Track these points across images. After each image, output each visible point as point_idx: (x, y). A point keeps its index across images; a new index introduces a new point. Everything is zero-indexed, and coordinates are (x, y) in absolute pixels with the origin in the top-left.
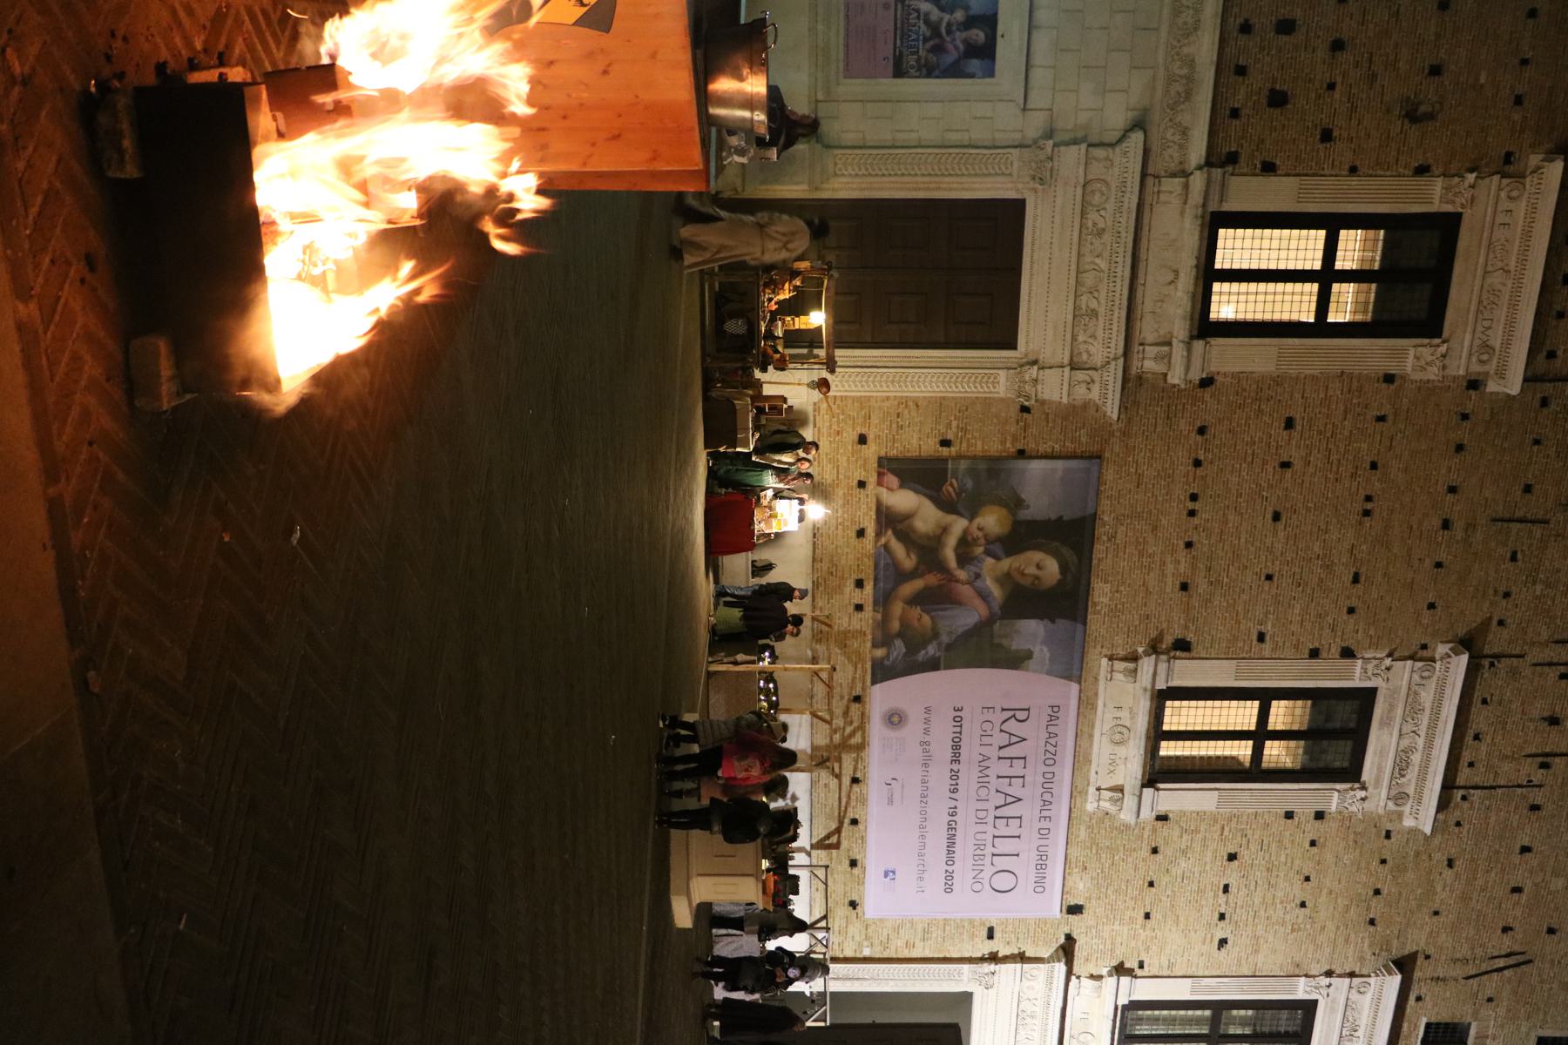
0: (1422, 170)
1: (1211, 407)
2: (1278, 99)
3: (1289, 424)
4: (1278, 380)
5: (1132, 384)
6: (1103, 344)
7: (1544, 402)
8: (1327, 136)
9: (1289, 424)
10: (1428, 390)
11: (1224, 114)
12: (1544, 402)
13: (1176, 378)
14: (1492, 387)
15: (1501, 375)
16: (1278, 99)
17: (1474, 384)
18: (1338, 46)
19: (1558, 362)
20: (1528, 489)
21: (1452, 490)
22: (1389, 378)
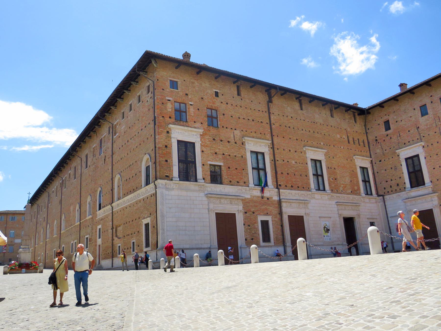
0: (401, 165)
1: (435, 180)
2: (398, 185)
3: (434, 168)
4: (429, 172)
5: (434, 192)
6: (428, 198)
7: (424, 137)
8: (400, 178)
9: (434, 168)
10: (426, 152)
11: (401, 191)
12: (424, 137)
13: (432, 186)
14: (423, 145)
15: (421, 145)
16: (398, 185)
17: (423, 147)
18: (391, 180)
19: (418, 138)
20: (435, 132)
21: (438, 142)
22: (425, 158)
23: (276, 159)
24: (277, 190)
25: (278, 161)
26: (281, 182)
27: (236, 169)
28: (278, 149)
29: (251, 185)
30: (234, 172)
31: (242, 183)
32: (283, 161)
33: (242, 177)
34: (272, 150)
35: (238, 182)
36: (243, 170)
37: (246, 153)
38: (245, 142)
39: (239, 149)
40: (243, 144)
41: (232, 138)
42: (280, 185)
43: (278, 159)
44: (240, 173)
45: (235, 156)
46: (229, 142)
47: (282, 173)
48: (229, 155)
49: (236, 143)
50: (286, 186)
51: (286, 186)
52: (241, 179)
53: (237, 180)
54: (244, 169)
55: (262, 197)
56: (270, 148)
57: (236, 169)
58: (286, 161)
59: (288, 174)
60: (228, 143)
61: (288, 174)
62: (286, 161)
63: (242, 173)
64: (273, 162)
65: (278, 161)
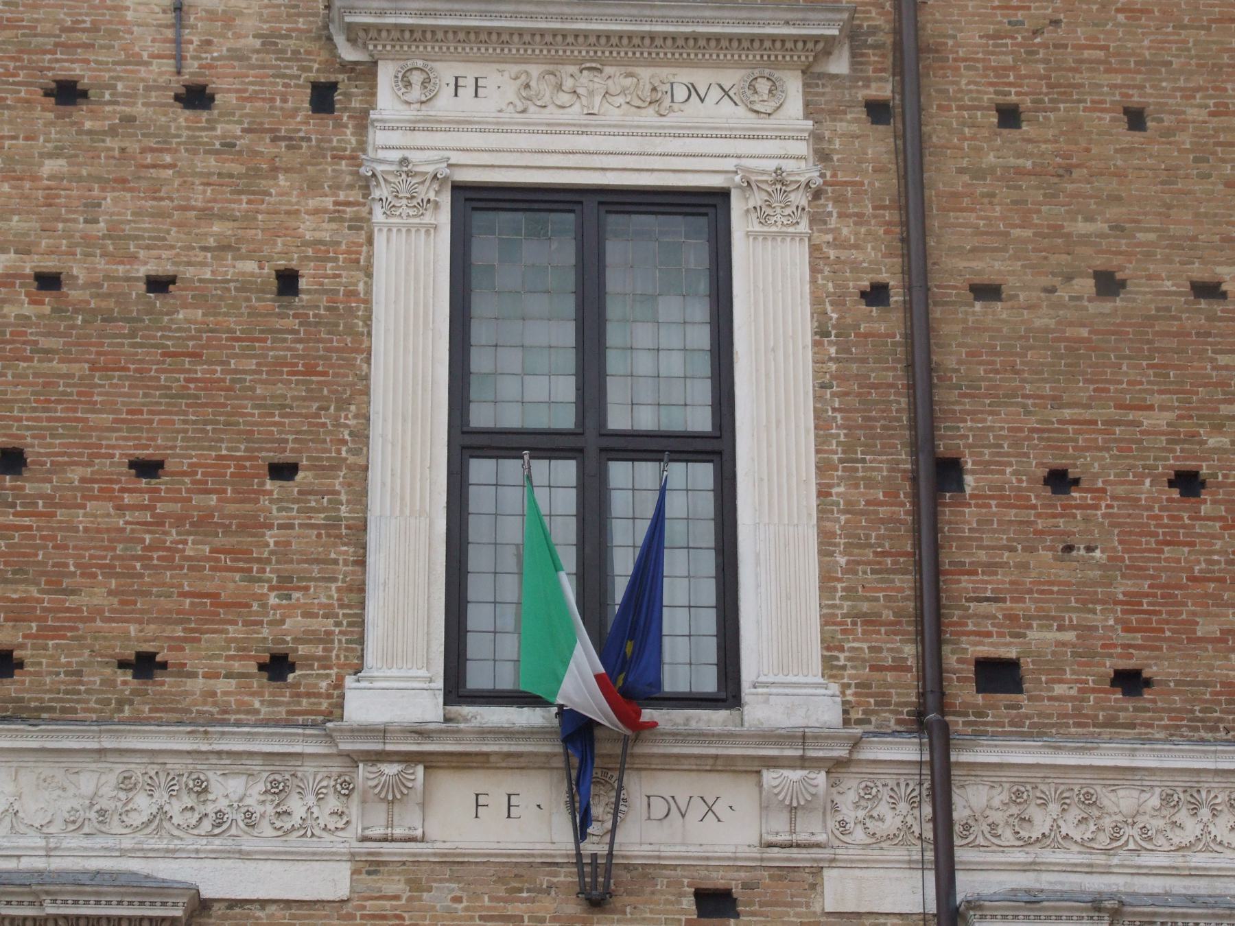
23: (956, 264)
24: (908, 751)
25: (987, 292)
26: (1016, 625)
27: (147, 468)
28: (1009, 116)
29: (395, 687)
30: (99, 512)
31: (213, 668)
32: (1108, 284)
33: (231, 585)
34: (878, 145)
35: (145, 665)
36: (283, 471)
37: (361, 224)
38: (366, 73)
39: (253, 180)
40: (323, 98)
41: (147, 42)
42: (998, 675)
43: (990, 268)
44: (203, 524)
45: (158, 285)
46: (67, 93)
47: (1059, 480)
48: (48, 282)
49: (196, 97)
50: (1130, 681)
51: (1130, 681)
52: (214, 609)
53: (136, 636)
54: (309, 463)
55: (598, 884)
56: (854, 122)
57: (147, 468)
58: (1158, 283)
59: (1188, 482)
60: (45, 113)
61: (1188, 482)
62: (1158, 283)
63: (254, 525)
64: (887, 324)
65: (987, 292)
